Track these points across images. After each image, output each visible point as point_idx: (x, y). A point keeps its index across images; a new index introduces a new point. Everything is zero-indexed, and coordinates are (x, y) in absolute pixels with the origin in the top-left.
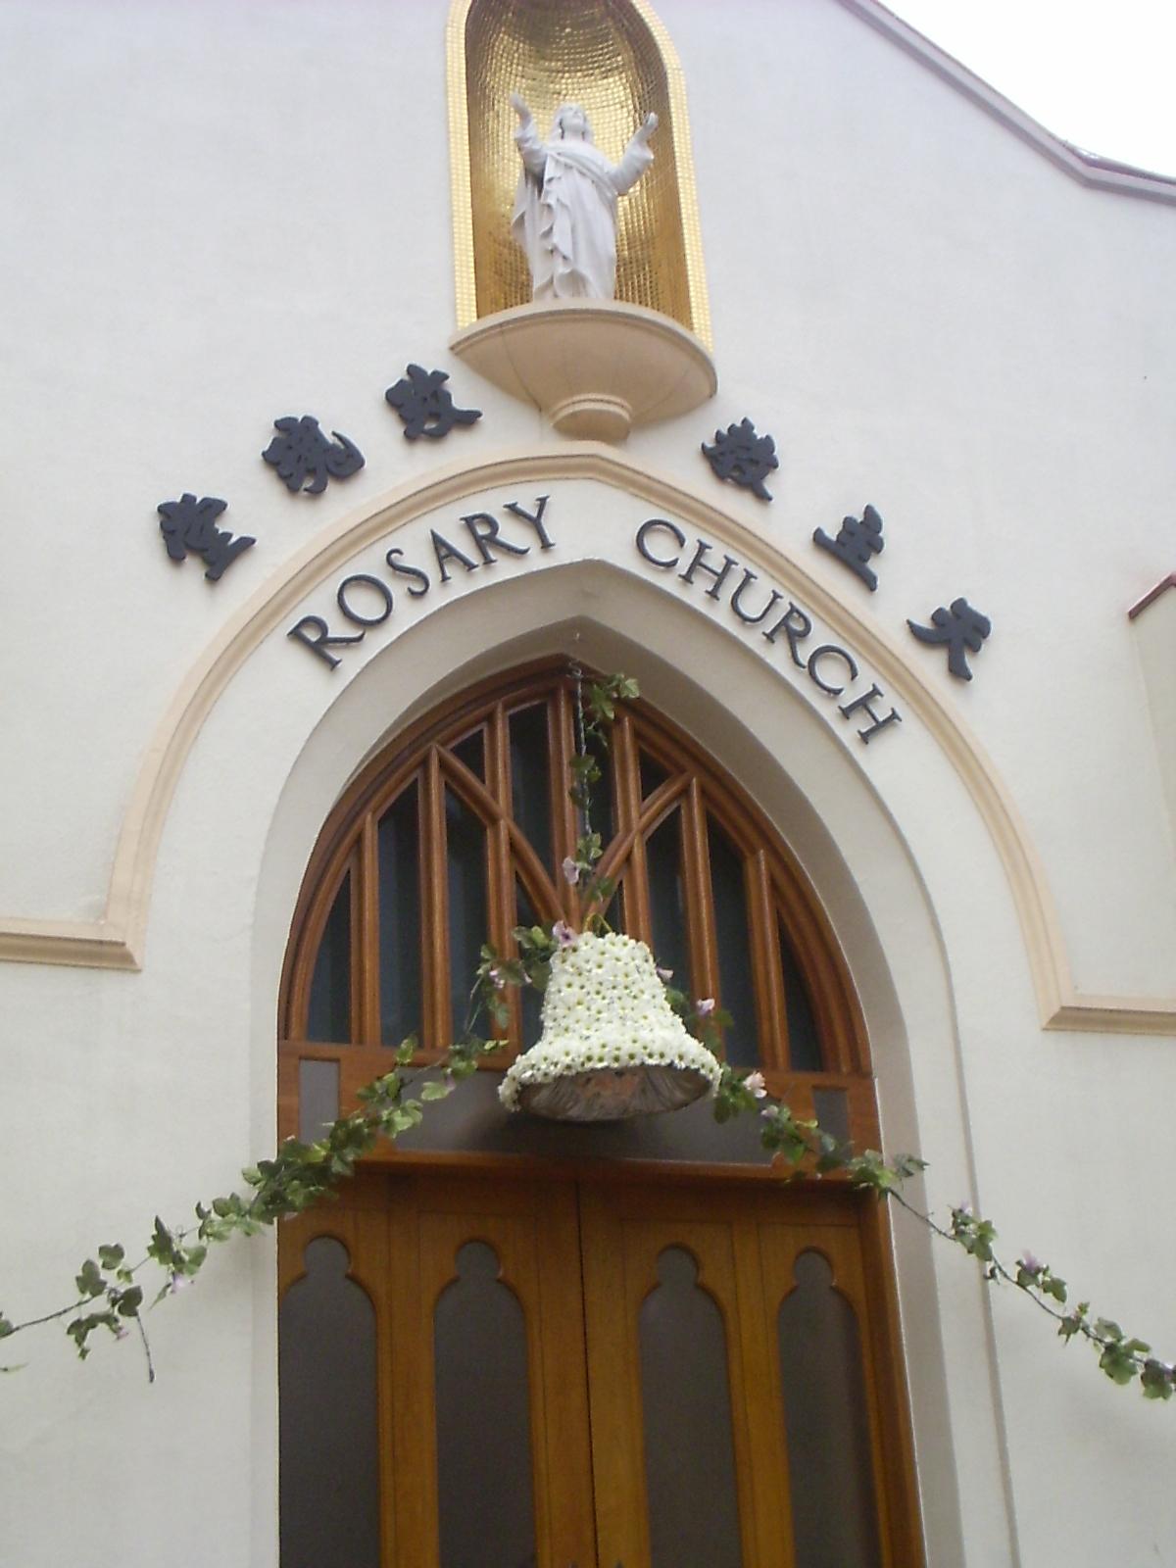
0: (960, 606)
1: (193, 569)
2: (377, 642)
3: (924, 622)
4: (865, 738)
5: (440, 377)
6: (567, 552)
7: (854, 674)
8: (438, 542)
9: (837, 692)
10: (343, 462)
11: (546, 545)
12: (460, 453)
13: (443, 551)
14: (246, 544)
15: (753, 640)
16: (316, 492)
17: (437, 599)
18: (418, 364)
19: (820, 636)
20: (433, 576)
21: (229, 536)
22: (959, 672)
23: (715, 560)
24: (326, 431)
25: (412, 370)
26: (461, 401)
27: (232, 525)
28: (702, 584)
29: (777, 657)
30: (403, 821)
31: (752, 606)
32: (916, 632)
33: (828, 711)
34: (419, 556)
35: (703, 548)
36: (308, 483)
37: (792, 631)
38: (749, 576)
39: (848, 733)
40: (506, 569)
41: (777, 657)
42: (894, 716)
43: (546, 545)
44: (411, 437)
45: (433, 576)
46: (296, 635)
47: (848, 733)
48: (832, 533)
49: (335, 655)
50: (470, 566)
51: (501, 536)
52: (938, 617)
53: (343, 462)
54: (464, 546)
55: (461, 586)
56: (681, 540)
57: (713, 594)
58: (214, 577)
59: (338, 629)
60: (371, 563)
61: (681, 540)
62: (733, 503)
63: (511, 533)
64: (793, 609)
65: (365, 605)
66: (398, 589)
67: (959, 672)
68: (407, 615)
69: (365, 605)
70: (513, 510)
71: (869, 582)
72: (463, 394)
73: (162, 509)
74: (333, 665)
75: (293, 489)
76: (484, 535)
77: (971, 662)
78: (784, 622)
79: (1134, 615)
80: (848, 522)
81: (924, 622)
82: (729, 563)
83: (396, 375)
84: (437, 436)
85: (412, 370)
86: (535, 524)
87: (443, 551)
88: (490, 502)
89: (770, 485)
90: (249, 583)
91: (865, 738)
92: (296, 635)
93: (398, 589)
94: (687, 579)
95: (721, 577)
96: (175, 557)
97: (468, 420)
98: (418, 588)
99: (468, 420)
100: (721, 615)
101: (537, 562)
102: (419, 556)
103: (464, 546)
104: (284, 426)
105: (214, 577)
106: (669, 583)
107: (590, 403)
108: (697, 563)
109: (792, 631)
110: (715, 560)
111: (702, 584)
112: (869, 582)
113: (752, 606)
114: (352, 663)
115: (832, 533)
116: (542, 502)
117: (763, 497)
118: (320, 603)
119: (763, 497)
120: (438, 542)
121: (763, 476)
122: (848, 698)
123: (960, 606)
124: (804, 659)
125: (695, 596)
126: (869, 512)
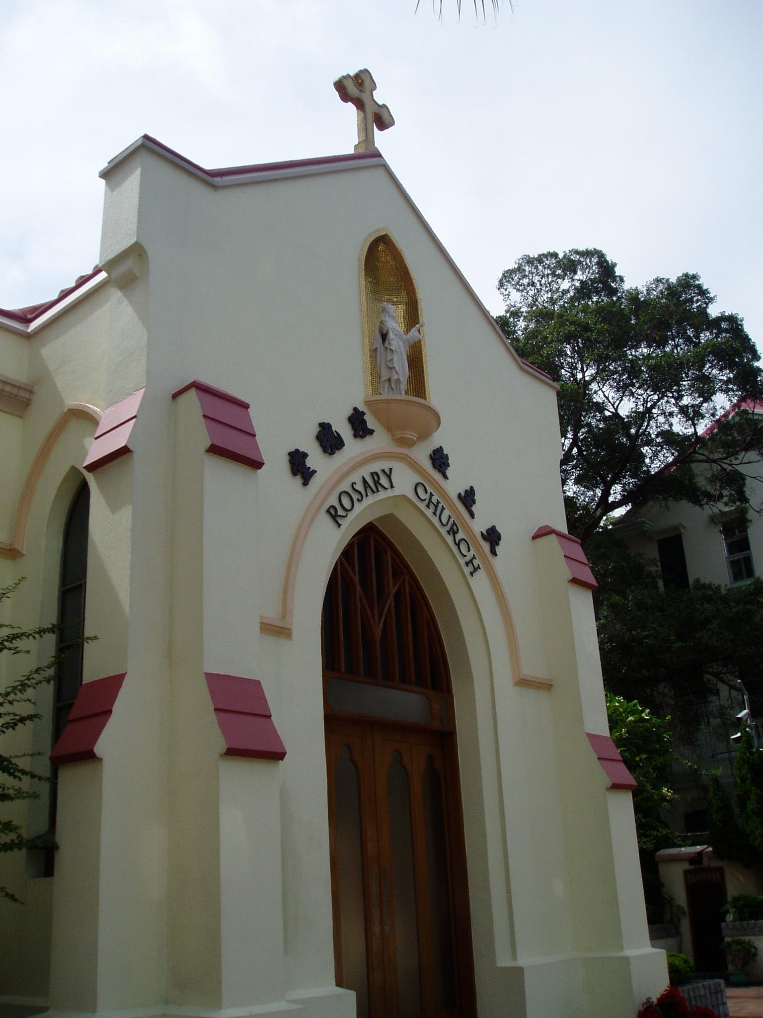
1: (298, 480)
6: (397, 491)
7: (469, 550)
18: (358, 408)
20: (364, 494)
21: (309, 468)
26: (370, 426)
37: (453, 531)
39: (467, 570)
41: (449, 539)
43: (392, 486)
45: (364, 494)
46: (328, 511)
47: (467, 570)
51: (381, 481)
58: (305, 483)
63: (384, 481)
72: (371, 422)
74: (339, 525)
75: (325, 451)
79: (535, 537)
82: (438, 502)
83: (350, 412)
84: (363, 437)
86: (389, 476)
92: (328, 511)
93: (355, 497)
97: (371, 432)
98: (360, 499)
99: (371, 432)
100: (435, 520)
102: (359, 487)
104: (322, 425)
106: (422, 506)
109: (453, 531)
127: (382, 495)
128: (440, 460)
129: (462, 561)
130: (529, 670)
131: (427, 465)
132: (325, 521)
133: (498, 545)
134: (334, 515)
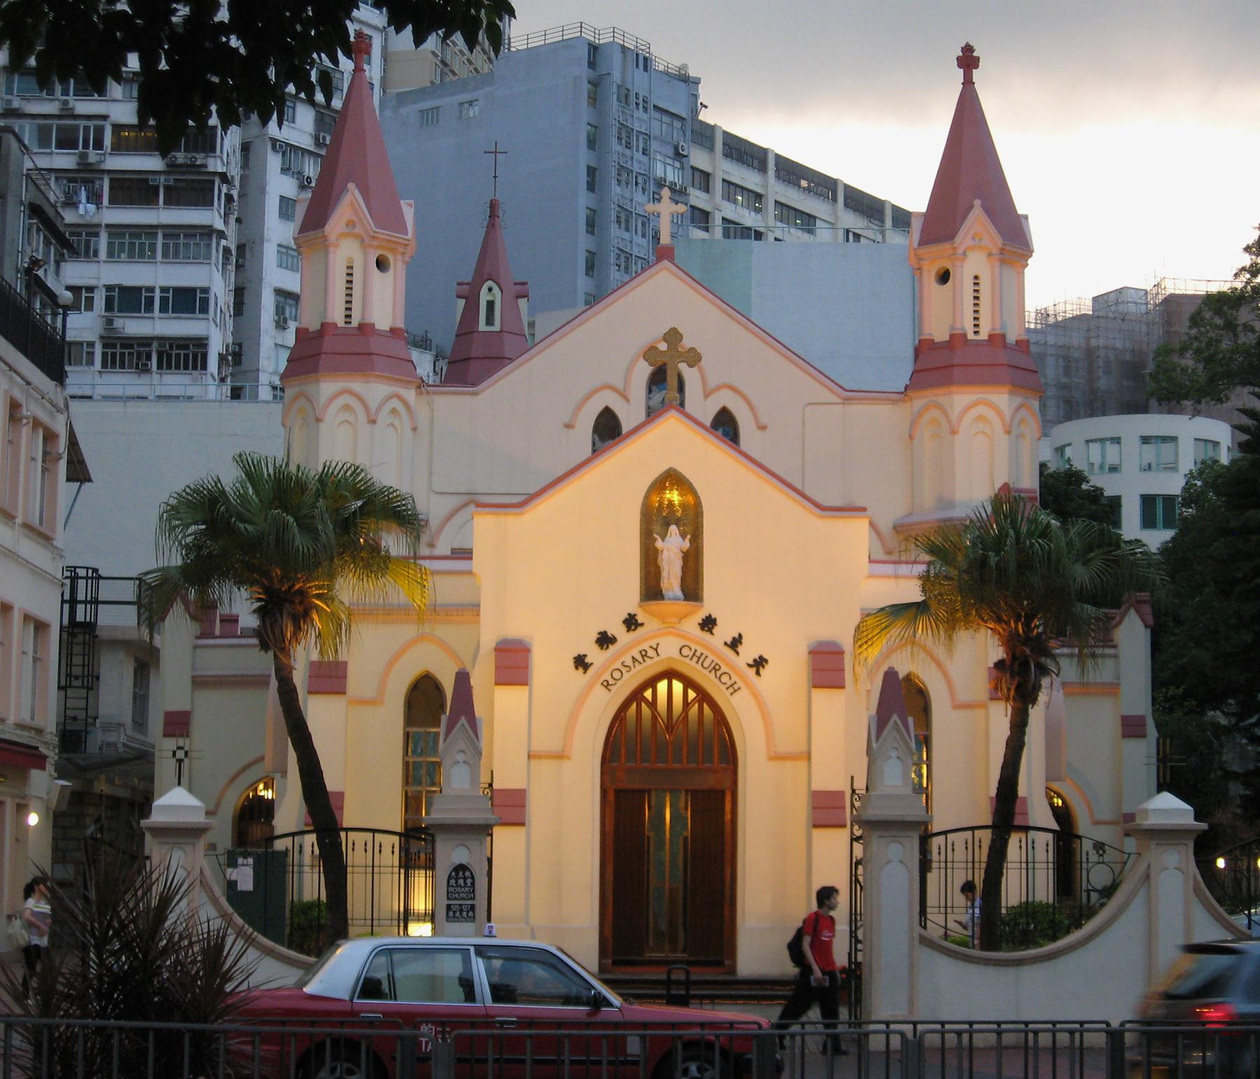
0: (761, 657)
1: (581, 670)
2: (619, 683)
3: (751, 662)
4: (731, 694)
5: (635, 615)
8: (633, 658)
9: (725, 684)
11: (658, 655)
14: (592, 664)
16: (608, 647)
19: (724, 669)
20: (632, 667)
22: (758, 673)
23: (698, 654)
24: (609, 634)
25: (629, 614)
26: (640, 621)
27: (587, 660)
28: (695, 659)
31: (706, 665)
32: (749, 665)
34: (629, 662)
35: (696, 651)
36: (605, 646)
37: (716, 669)
38: (706, 657)
39: (728, 693)
42: (739, 688)
43: (658, 655)
44: (628, 631)
45: (632, 667)
46: (602, 684)
47: (728, 693)
48: (729, 642)
49: (610, 687)
50: (640, 663)
52: (755, 661)
54: (639, 658)
56: (691, 649)
57: (697, 662)
59: (611, 682)
60: (618, 665)
61: (691, 649)
63: (651, 653)
64: (717, 664)
66: (624, 670)
67: (758, 673)
70: (651, 647)
71: (737, 653)
73: (575, 658)
74: (610, 690)
75: (602, 648)
76: (644, 655)
77: (762, 671)
78: (714, 668)
80: (734, 638)
81: (751, 662)
82: (702, 654)
83: (625, 616)
84: (636, 629)
85: (629, 614)
86: (656, 650)
88: (645, 646)
89: (714, 631)
90: (591, 671)
91: (731, 694)
93: (624, 670)
94: (691, 659)
95: (699, 658)
96: (577, 668)
97: (642, 625)
99: (642, 625)
102: (629, 662)
103: (639, 658)
105: (585, 672)
108: (694, 654)
110: (698, 654)
111: (695, 659)
112: (737, 653)
115: (729, 642)
116: (658, 644)
117: (712, 633)
118: (607, 676)
119: (712, 633)
120: (633, 658)
121: (713, 627)
122: (729, 683)
123: (761, 657)
124: (718, 676)
126: (740, 636)
127: (649, 661)
129: (723, 687)
130: (785, 744)
131: (697, 631)
132: (599, 690)
133: (763, 667)
134: (607, 685)
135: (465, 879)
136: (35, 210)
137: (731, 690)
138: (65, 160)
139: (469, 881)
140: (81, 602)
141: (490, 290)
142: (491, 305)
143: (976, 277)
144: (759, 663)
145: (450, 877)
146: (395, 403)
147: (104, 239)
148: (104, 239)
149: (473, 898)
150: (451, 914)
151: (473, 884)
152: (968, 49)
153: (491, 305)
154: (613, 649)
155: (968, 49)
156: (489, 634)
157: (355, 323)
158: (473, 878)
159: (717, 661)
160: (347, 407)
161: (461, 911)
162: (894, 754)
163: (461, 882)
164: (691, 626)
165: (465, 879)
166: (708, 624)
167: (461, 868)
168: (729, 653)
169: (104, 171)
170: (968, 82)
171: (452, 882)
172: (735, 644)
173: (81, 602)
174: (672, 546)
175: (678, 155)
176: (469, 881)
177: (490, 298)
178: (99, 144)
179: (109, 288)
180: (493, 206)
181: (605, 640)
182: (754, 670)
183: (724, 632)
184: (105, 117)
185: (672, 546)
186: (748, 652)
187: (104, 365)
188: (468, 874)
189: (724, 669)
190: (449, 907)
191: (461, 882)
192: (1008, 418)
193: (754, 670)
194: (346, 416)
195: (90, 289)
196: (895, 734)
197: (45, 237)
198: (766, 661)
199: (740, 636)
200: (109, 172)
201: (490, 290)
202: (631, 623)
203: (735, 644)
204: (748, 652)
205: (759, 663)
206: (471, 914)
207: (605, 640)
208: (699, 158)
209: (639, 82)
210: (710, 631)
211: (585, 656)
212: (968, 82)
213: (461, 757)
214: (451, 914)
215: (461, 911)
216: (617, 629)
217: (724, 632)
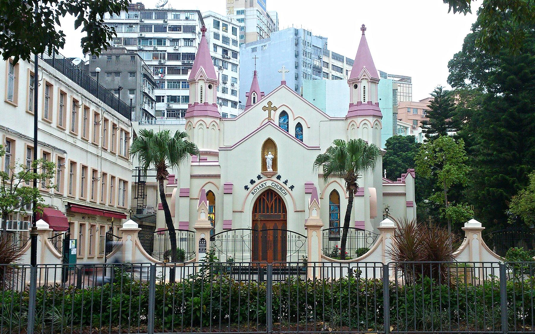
0: (292, 185)
1: (246, 190)
2: (256, 193)
10: (255, 182)
12: (261, 180)
13: (260, 187)
15: (278, 190)
17: (260, 190)
19: (283, 189)
22: (292, 190)
28: (275, 186)
29: (280, 191)
30: (260, 200)
31: (278, 188)
33: (283, 194)
40: (264, 187)
53: (255, 182)
55: (261, 189)
59: (254, 192)
60: (256, 188)
62: (278, 181)
63: (264, 185)
65: (255, 191)
66: (257, 189)
67: (292, 190)
68: (258, 191)
69: (255, 191)
71: (286, 185)
77: (293, 189)
87: (260, 187)
90: (249, 190)
93: (257, 189)
97: (262, 178)
99: (262, 178)
100: (276, 188)
101: (266, 186)
106: (273, 187)
107: (268, 176)
111: (275, 186)
112: (286, 185)
113: (278, 188)
114: (255, 194)
118: (253, 191)
122: (284, 192)
123: (292, 185)
125: (275, 187)
126: (287, 180)
128: (279, 177)
129: (283, 194)
132: (251, 194)
134: (253, 193)
135: (204, 242)
136: (145, 76)
137: (285, 194)
138: (156, 63)
139: (205, 242)
140: (137, 176)
141: (254, 94)
142: (254, 98)
143: (364, 87)
144: (292, 187)
145: (200, 242)
146: (214, 123)
147: (166, 83)
148: (166, 83)
149: (206, 247)
150: (200, 251)
151: (206, 243)
152: (363, 25)
153: (254, 98)
154: (255, 184)
155: (363, 25)
156: (222, 181)
157: (203, 102)
158: (206, 241)
159: (281, 187)
160: (201, 124)
161: (203, 250)
162: (315, 208)
163: (203, 243)
164: (274, 178)
165: (204, 242)
166: (279, 177)
167: (203, 239)
168: (284, 185)
169: (165, 65)
170: (363, 34)
171: (200, 243)
172: (286, 182)
173: (137, 176)
174: (270, 157)
175: (320, 58)
176: (205, 242)
177: (254, 96)
178: (164, 58)
179: (168, 96)
180: (255, 72)
181: (252, 182)
182: (291, 189)
183: (283, 179)
184: (165, 51)
185: (270, 157)
186: (289, 184)
187: (167, 116)
188: (204, 241)
189: (283, 189)
190: (200, 249)
191: (203, 243)
192: (372, 124)
193: (291, 189)
194: (201, 126)
195: (163, 97)
196: (315, 203)
197: (148, 83)
198: (294, 187)
199: (287, 180)
200: (167, 65)
201: (254, 94)
202: (259, 177)
203: (286, 182)
204: (289, 184)
205: (292, 187)
206: (205, 251)
207: (252, 182)
208: (325, 59)
209: (308, 39)
210: (279, 179)
211: (247, 186)
212: (363, 34)
213: (203, 211)
214: (200, 251)
215: (203, 250)
216: (255, 179)
217: (283, 179)
